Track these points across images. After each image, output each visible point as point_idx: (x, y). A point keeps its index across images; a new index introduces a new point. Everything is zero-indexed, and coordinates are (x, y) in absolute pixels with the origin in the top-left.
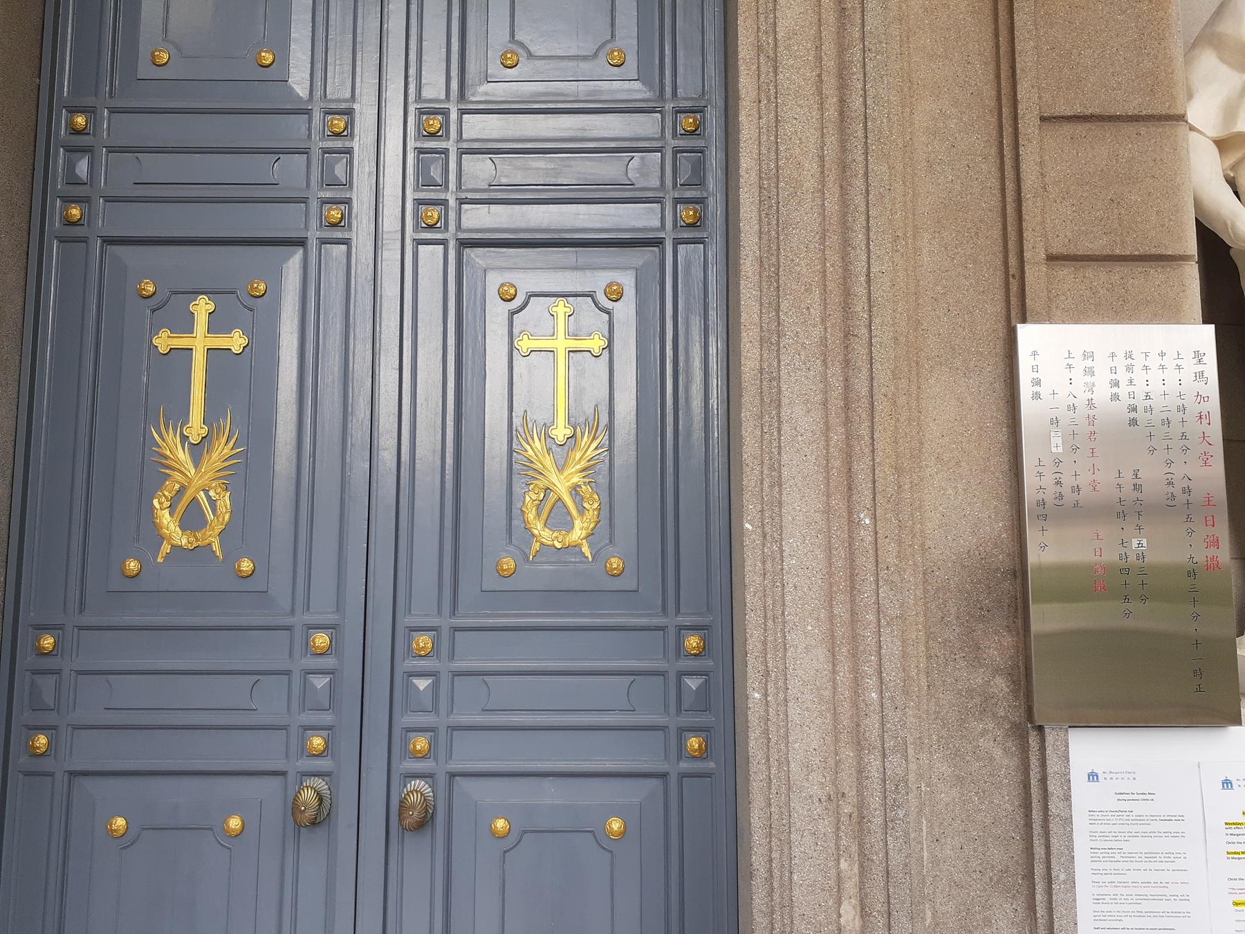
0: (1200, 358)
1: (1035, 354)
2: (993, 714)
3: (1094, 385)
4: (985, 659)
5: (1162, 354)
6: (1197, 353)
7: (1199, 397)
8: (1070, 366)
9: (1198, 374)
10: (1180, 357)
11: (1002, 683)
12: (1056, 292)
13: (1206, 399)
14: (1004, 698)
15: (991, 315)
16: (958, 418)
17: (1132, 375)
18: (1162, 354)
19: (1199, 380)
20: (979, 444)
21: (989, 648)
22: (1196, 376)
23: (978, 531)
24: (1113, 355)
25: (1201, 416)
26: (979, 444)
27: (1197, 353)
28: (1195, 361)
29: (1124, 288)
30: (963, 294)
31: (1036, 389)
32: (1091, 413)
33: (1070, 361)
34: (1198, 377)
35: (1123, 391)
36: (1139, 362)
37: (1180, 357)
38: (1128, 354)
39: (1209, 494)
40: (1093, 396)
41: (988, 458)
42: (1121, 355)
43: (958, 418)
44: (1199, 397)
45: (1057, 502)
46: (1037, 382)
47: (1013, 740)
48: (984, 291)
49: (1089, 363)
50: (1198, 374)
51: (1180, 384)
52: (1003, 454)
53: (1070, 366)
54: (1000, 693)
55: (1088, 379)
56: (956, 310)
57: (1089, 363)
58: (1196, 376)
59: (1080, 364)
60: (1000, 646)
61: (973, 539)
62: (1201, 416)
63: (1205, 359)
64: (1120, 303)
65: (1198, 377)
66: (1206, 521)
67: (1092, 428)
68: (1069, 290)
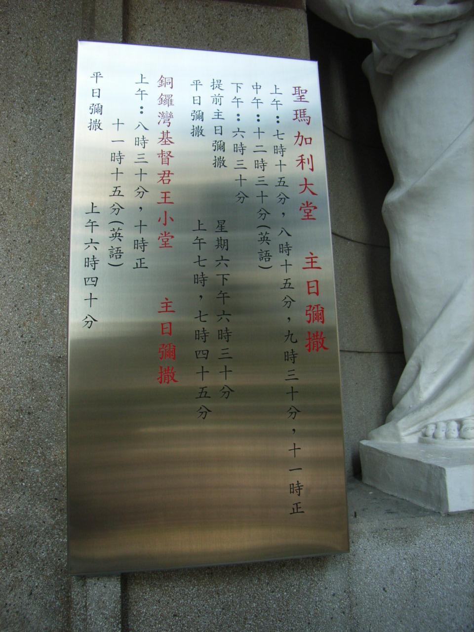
0: (301, 95)
1: (97, 75)
2: (31, 557)
3: (171, 116)
4: (22, 480)
5: (257, 87)
6: (297, 90)
7: (300, 138)
8: (142, 93)
9: (298, 112)
10: (278, 91)
11: (44, 513)
12: (142, 21)
13: (308, 141)
14: (47, 533)
15: (62, 43)
16: (8, 160)
17: (221, 109)
18: (257, 87)
19: (300, 119)
20: (33, 193)
21: (29, 464)
22: (297, 114)
23: (22, 304)
24: (197, 83)
25: (302, 160)
26: (33, 193)
27: (297, 90)
28: (295, 97)
29: (222, 25)
30: (29, 16)
31: (96, 116)
32: (166, 148)
33: (143, 87)
34: (299, 116)
35: (208, 124)
36: (228, 93)
37: (278, 91)
38: (216, 83)
39: (312, 254)
40: (169, 129)
41: (43, 211)
42: (207, 83)
43: (8, 160)
44: (300, 138)
45: (114, 261)
46: (99, 109)
47: (57, 592)
48: (55, 16)
49: (167, 90)
50: (298, 112)
51: (278, 122)
52: (63, 206)
53: (142, 93)
54: (41, 526)
55: (164, 108)
56: (17, 34)
57: (167, 90)
58: (297, 114)
59: (154, 91)
60: (44, 460)
61: (14, 316)
62: (302, 160)
63: (307, 97)
64: (217, 40)
65: (299, 116)
66: (309, 287)
67: (165, 167)
68: (158, 21)
